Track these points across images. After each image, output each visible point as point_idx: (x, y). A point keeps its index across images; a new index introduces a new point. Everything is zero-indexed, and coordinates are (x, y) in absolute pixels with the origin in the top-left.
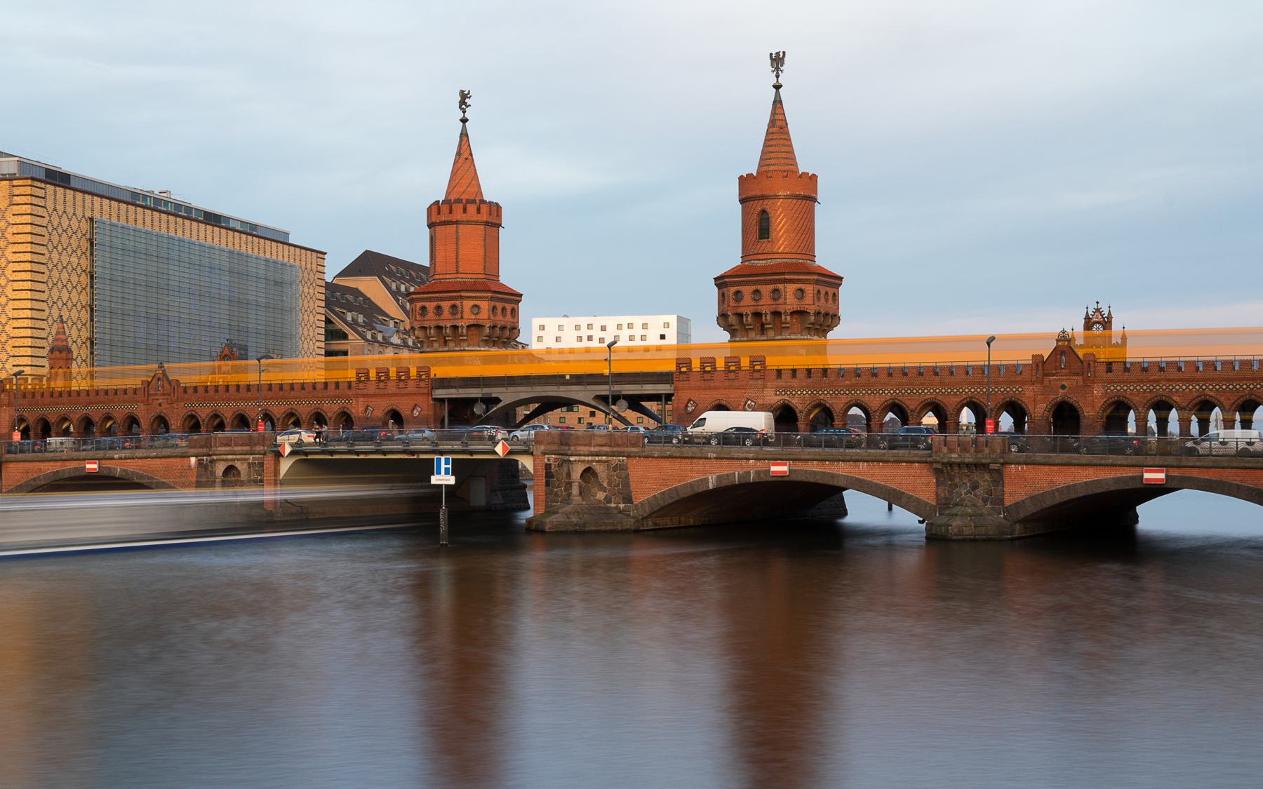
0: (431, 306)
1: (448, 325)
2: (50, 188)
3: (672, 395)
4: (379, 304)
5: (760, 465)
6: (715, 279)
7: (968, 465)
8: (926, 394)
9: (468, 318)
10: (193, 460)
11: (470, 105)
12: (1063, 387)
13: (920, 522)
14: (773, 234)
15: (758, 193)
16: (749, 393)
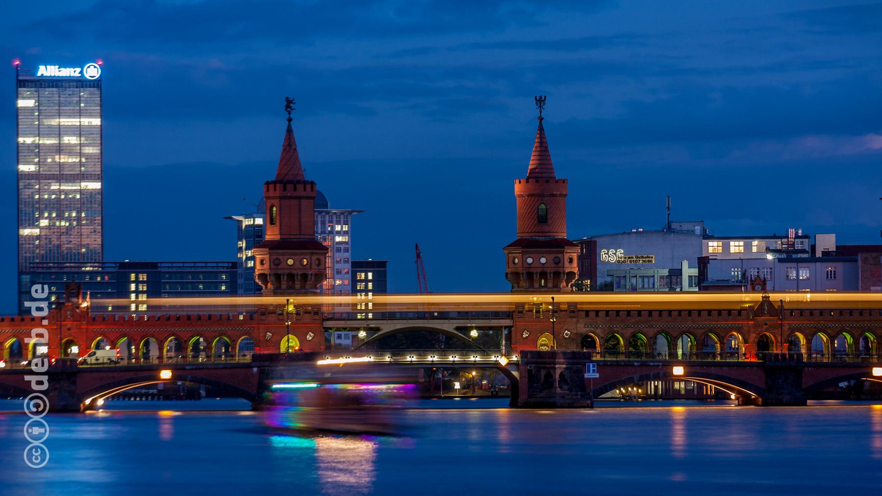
1: (300, 273)
3: (511, 327)
8: (683, 327)
10: (255, 369)
11: (294, 109)
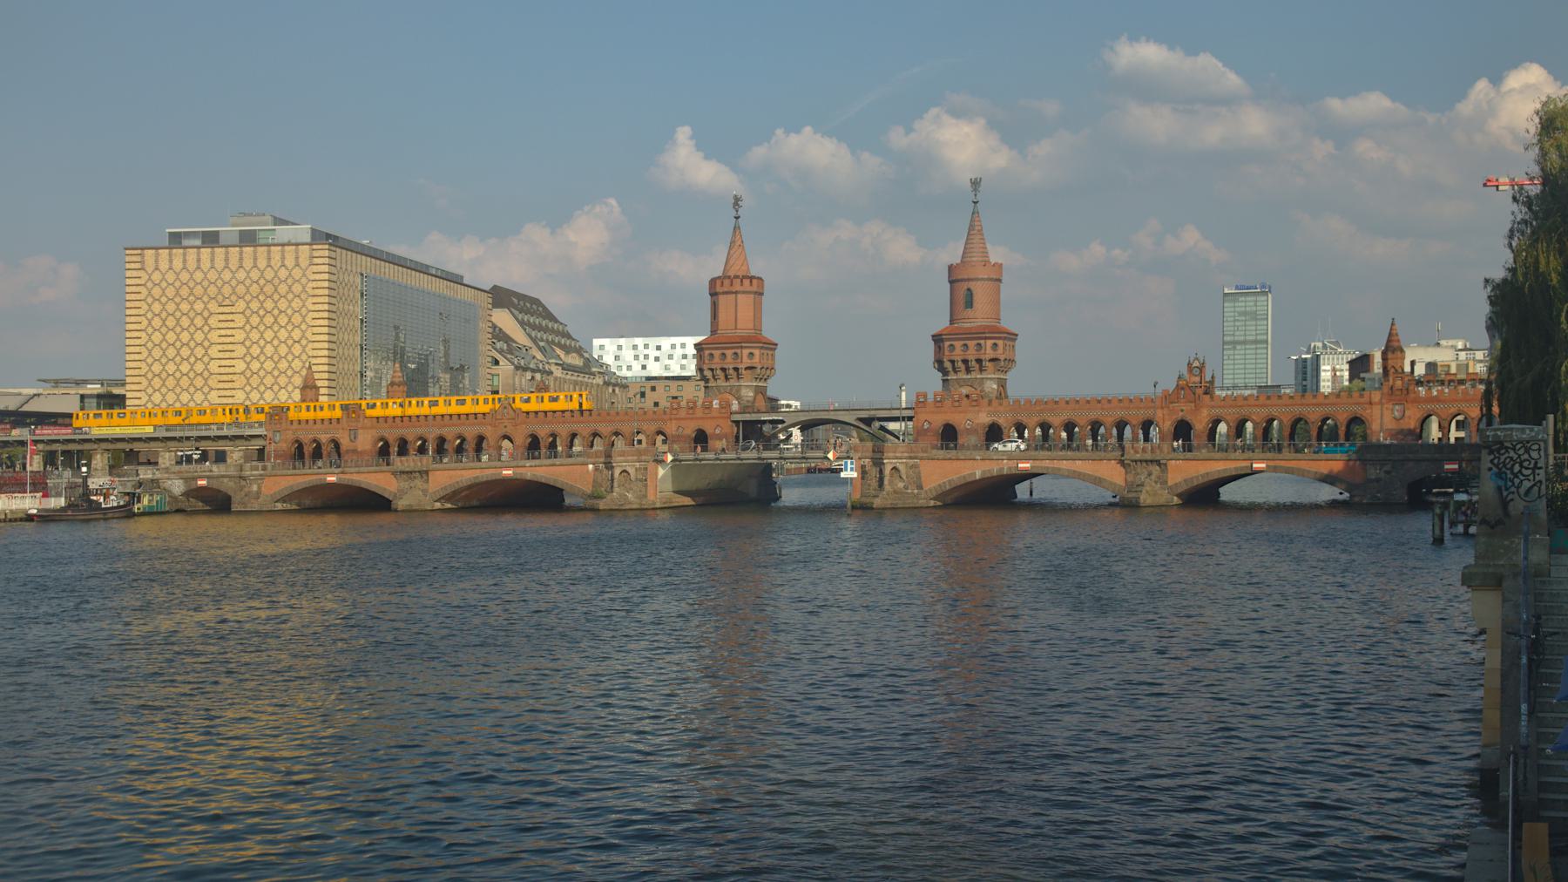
0: (717, 353)
1: (731, 367)
2: (338, 250)
4: (508, 332)
5: (1012, 463)
6: (933, 336)
7: (1146, 461)
9: (747, 362)
10: (591, 466)
12: (1182, 411)
13: (1114, 497)
14: (975, 304)
15: (966, 277)
16: (969, 416)
